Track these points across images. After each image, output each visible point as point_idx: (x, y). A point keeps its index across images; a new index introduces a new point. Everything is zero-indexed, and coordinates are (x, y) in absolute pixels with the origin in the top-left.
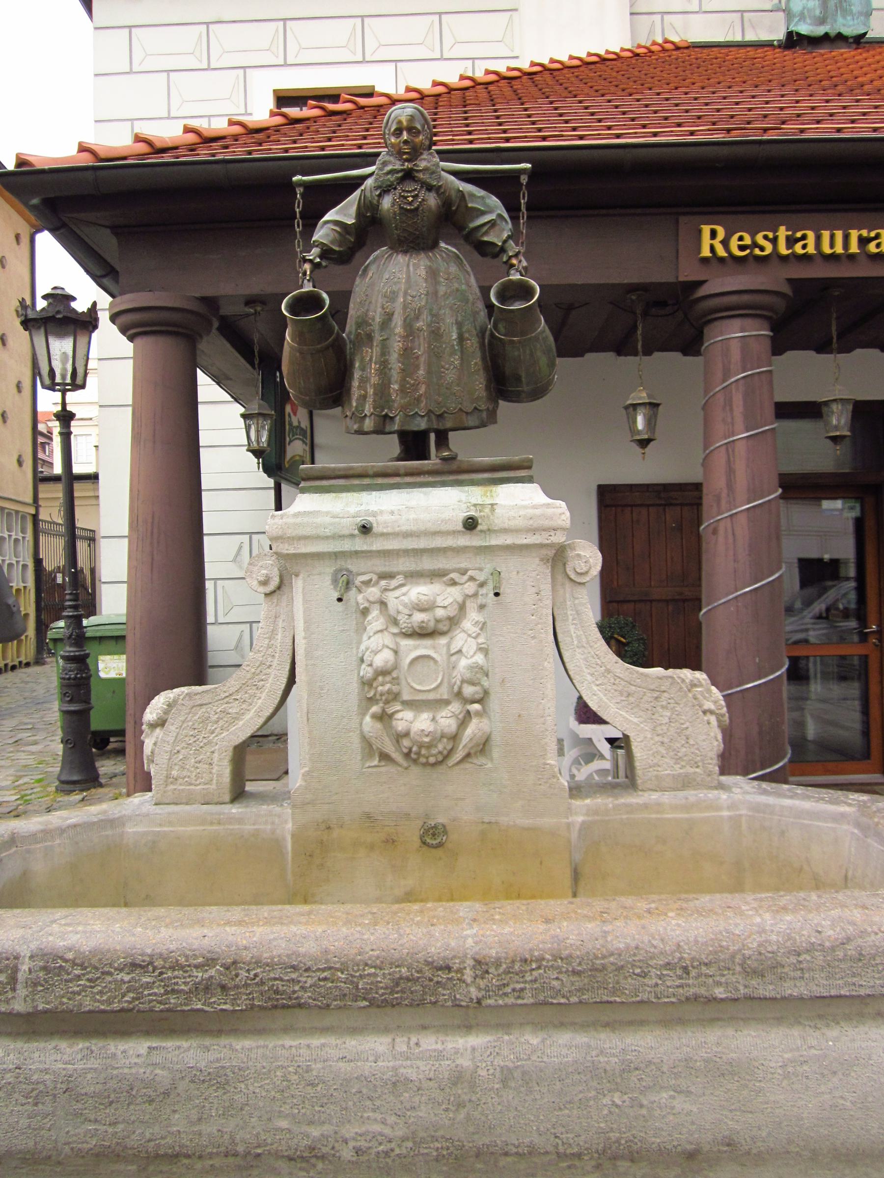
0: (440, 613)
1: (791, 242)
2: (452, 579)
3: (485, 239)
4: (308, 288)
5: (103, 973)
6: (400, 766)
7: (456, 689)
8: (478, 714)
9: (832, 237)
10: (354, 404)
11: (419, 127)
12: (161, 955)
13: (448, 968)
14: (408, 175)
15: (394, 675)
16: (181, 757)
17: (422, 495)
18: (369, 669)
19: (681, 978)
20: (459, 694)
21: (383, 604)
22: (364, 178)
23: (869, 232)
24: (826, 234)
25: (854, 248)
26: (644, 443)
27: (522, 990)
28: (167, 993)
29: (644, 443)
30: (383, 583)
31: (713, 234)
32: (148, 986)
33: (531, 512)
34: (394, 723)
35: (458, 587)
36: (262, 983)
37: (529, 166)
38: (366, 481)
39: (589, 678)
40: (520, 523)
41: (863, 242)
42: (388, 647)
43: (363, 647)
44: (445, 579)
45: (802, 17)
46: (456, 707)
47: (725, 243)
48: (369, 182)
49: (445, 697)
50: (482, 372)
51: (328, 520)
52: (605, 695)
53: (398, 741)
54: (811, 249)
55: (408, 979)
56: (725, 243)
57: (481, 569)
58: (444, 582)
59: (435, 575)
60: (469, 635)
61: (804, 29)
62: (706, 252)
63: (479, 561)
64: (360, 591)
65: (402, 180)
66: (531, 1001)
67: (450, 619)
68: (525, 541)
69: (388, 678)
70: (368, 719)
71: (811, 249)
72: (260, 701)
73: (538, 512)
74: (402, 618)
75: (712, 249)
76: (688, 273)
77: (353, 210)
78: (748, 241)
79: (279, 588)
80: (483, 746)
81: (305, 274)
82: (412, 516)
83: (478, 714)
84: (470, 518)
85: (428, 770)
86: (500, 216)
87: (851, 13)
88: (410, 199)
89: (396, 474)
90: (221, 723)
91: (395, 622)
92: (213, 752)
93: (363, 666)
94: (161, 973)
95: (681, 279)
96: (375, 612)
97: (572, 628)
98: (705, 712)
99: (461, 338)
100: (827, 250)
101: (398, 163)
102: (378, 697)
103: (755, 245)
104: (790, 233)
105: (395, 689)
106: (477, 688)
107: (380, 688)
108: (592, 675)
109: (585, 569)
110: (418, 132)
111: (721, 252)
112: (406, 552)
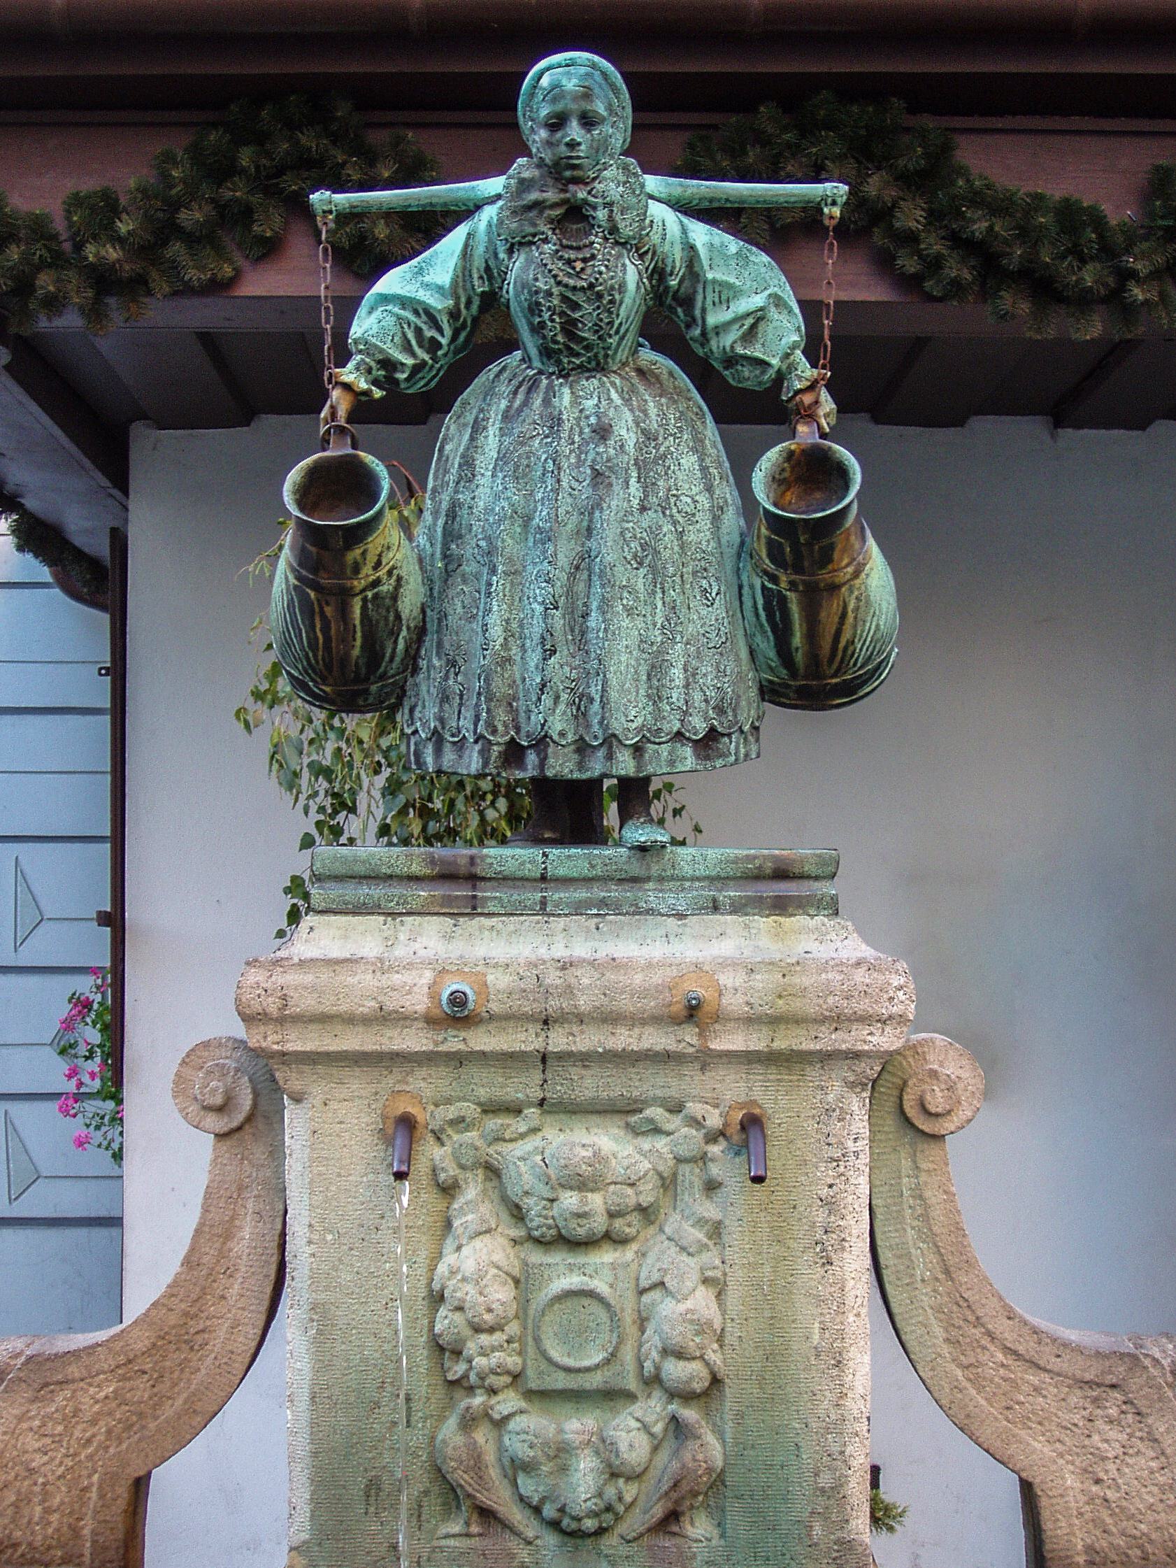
2: (651, 1121)
21: (493, 1171)
30: (493, 1123)
37: (844, 188)
44: (633, 1119)
48: (489, 213)
58: (627, 1125)
67: (642, 1210)
74: (533, 1206)
86: (777, 301)
88: (579, 265)
91: (518, 1213)
93: (442, 1312)
96: (471, 1192)
106: (695, 1367)
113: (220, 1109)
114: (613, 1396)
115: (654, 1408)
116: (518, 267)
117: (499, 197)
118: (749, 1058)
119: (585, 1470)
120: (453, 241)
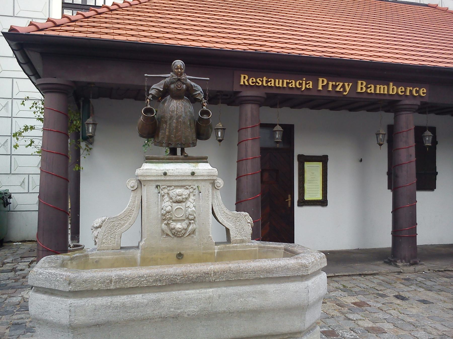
0: (184, 196)
1: (267, 82)
2: (187, 188)
3: (197, 98)
4: (149, 106)
5: (133, 279)
6: (172, 237)
7: (187, 217)
8: (193, 223)
9: (279, 81)
10: (160, 139)
11: (182, 68)
12: (146, 274)
13: (208, 274)
14: (179, 80)
15: (171, 213)
16: (106, 236)
17: (179, 165)
18: (165, 211)
19: (254, 274)
20: (188, 218)
21: (168, 194)
22: (165, 78)
23: (289, 81)
24: (277, 81)
25: (285, 85)
26: (220, 141)
27: (223, 277)
28: (147, 282)
29: (220, 141)
30: (169, 188)
31: (244, 78)
32: (143, 281)
33: (208, 171)
34: (170, 226)
35: (188, 190)
36: (169, 279)
38: (164, 161)
39: (220, 214)
40: (205, 174)
41: (288, 83)
42: (170, 205)
43: (163, 205)
44: (185, 187)
46: (187, 221)
47: (248, 81)
49: (184, 219)
50: (195, 133)
51: (155, 171)
52: (223, 218)
53: (171, 231)
54: (273, 85)
55: (200, 276)
56: (248, 81)
57: (194, 185)
58: (185, 188)
60: (191, 203)
62: (242, 83)
63: (195, 183)
64: (162, 190)
65: (177, 81)
66: (225, 280)
67: (186, 198)
68: (206, 178)
69: (170, 214)
70: (163, 225)
71: (273, 85)
72: (130, 220)
73: (210, 171)
75: (244, 82)
76: (236, 89)
77: (162, 86)
78: (254, 81)
79: (137, 189)
80: (193, 232)
81: (148, 102)
82: (177, 171)
83: (193, 223)
84: (193, 172)
85: (179, 238)
89: (172, 159)
90: (118, 226)
92: (116, 235)
93: (163, 210)
94: (146, 278)
95: (234, 90)
96: (166, 196)
97: (216, 201)
98: (248, 223)
99: (190, 124)
100: (277, 85)
101: (176, 76)
102: (166, 219)
103: (257, 82)
104: (267, 79)
105: (171, 217)
106: (193, 216)
107: (167, 216)
108: (220, 213)
109: (219, 186)
110: (182, 69)
111: (247, 83)
112: (175, 180)
113: (131, 187)
115: (187, 221)
117: (169, 77)
120: (163, 82)
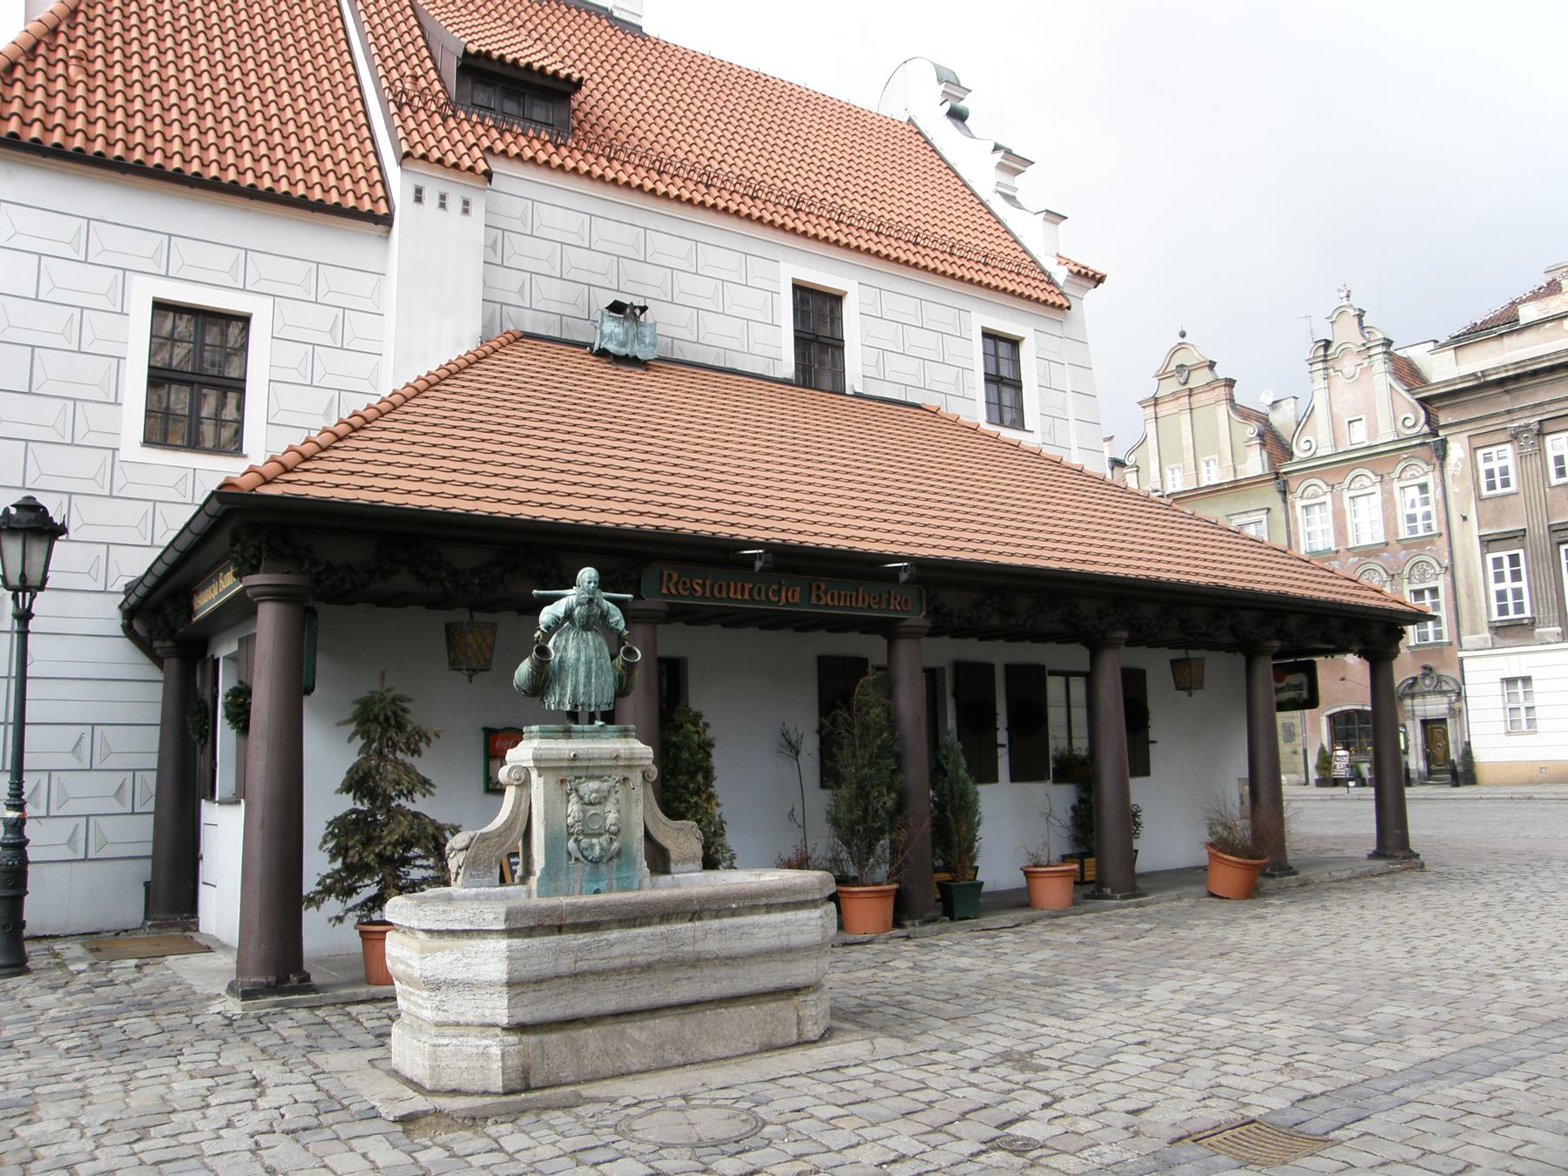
21: (577, 791)
45: (610, 337)
59: (599, 778)
61: (612, 347)
87: (644, 342)
114: (599, 835)
115: (607, 836)
116: (577, 610)
118: (625, 766)
119: (597, 848)
